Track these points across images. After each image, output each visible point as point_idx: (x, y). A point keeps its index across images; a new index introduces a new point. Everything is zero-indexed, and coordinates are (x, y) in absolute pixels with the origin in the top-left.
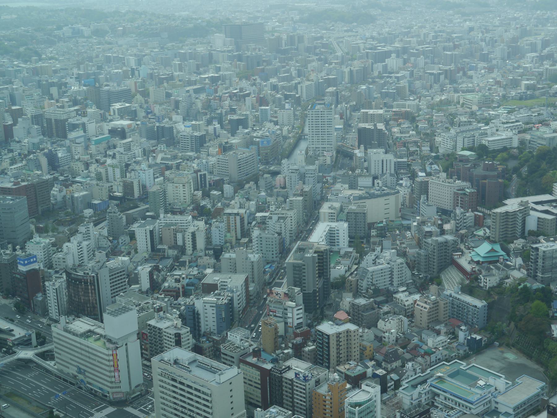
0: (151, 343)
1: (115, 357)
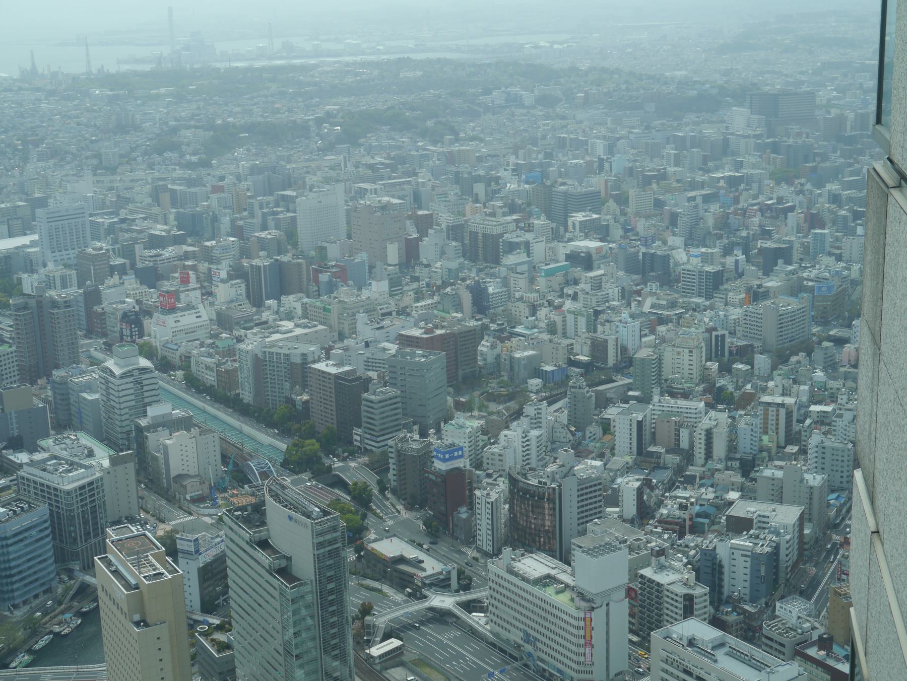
0: (648, 609)
1: (588, 623)
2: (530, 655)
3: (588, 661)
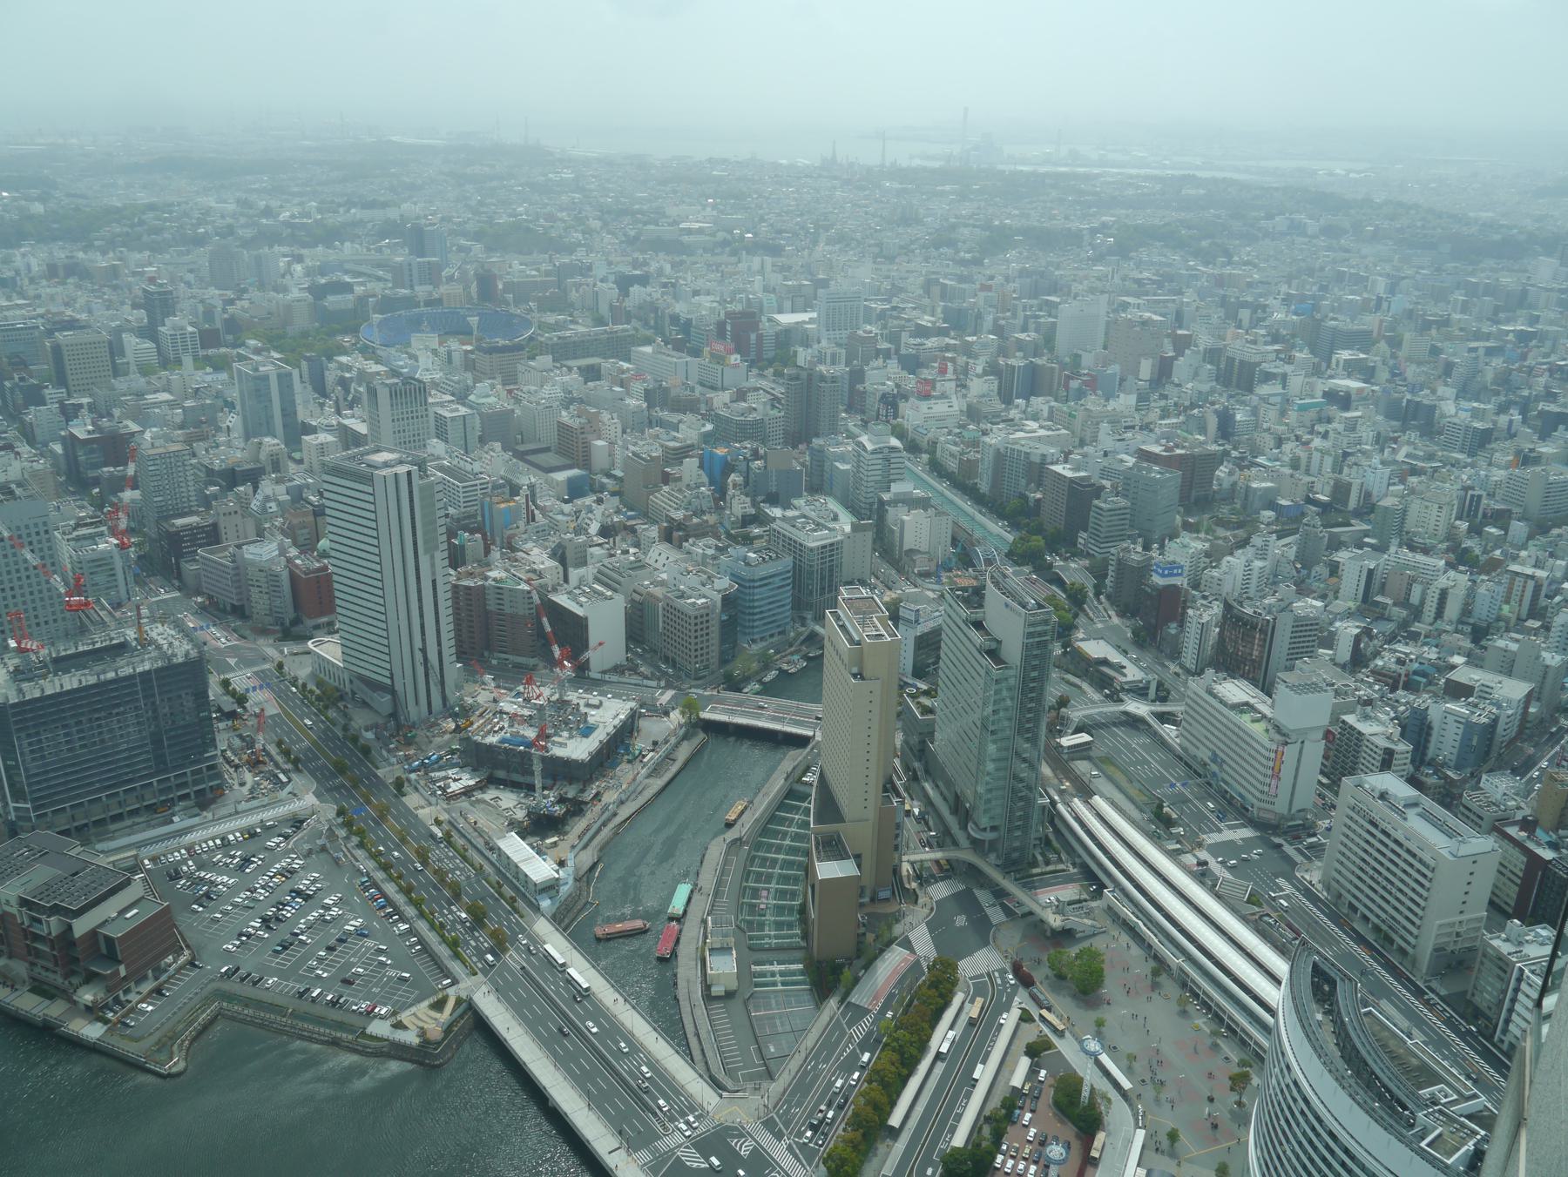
0: (1343, 754)
2: (1214, 774)
3: (1273, 792)
